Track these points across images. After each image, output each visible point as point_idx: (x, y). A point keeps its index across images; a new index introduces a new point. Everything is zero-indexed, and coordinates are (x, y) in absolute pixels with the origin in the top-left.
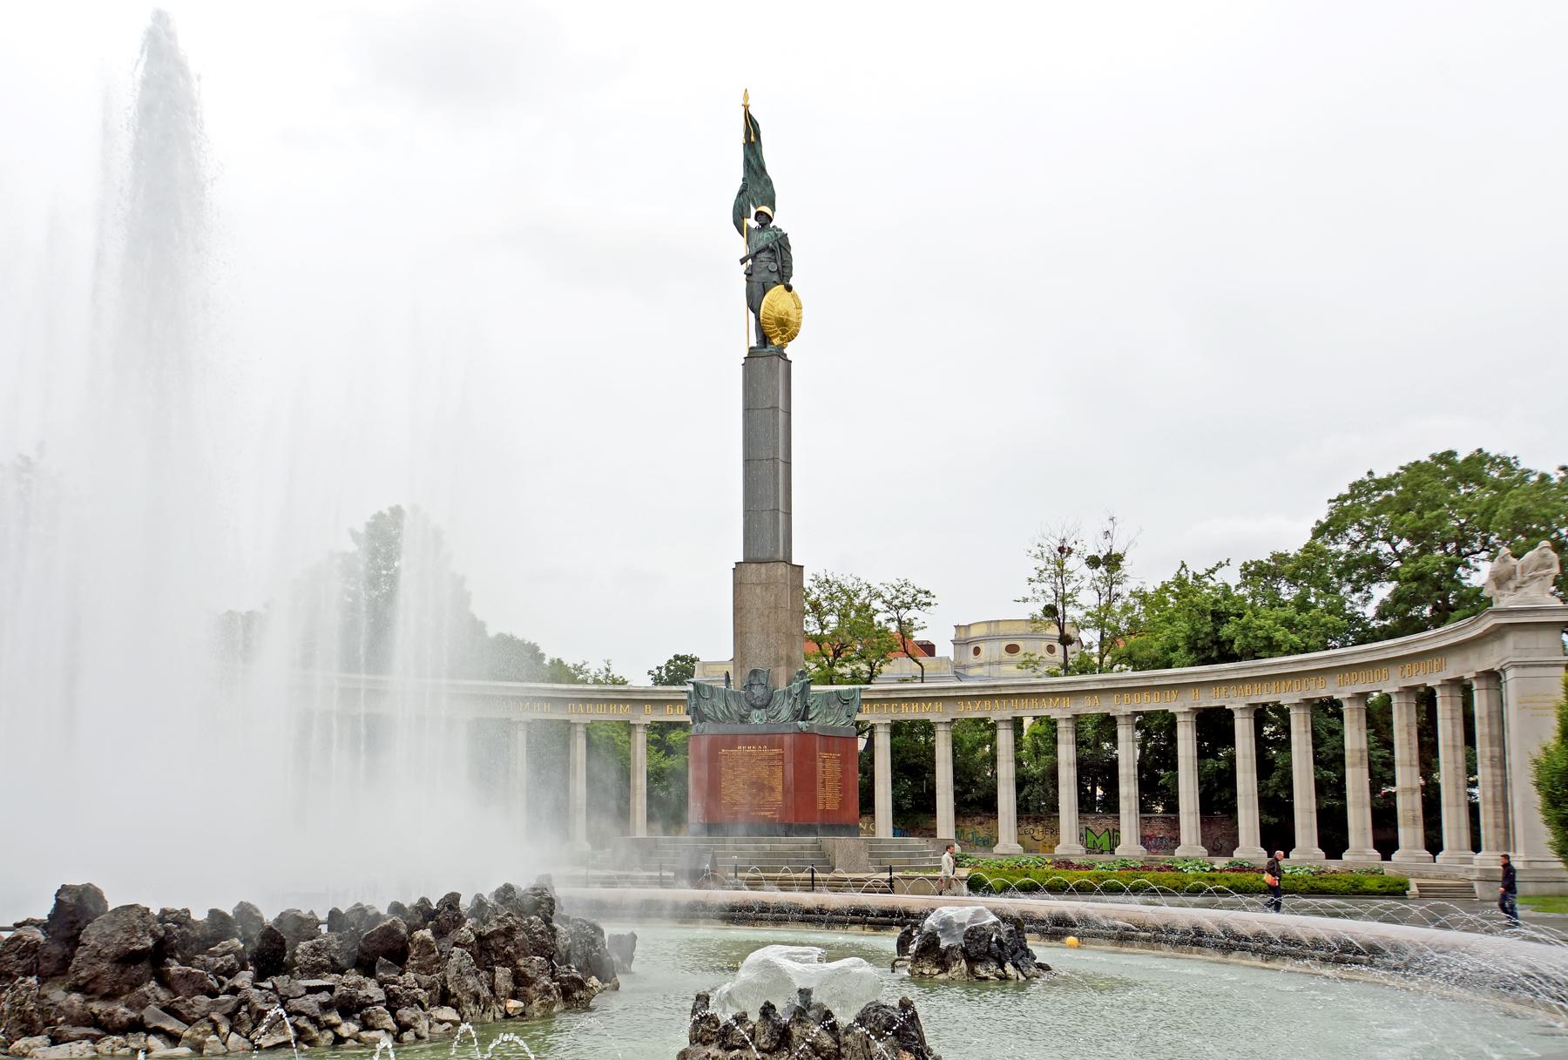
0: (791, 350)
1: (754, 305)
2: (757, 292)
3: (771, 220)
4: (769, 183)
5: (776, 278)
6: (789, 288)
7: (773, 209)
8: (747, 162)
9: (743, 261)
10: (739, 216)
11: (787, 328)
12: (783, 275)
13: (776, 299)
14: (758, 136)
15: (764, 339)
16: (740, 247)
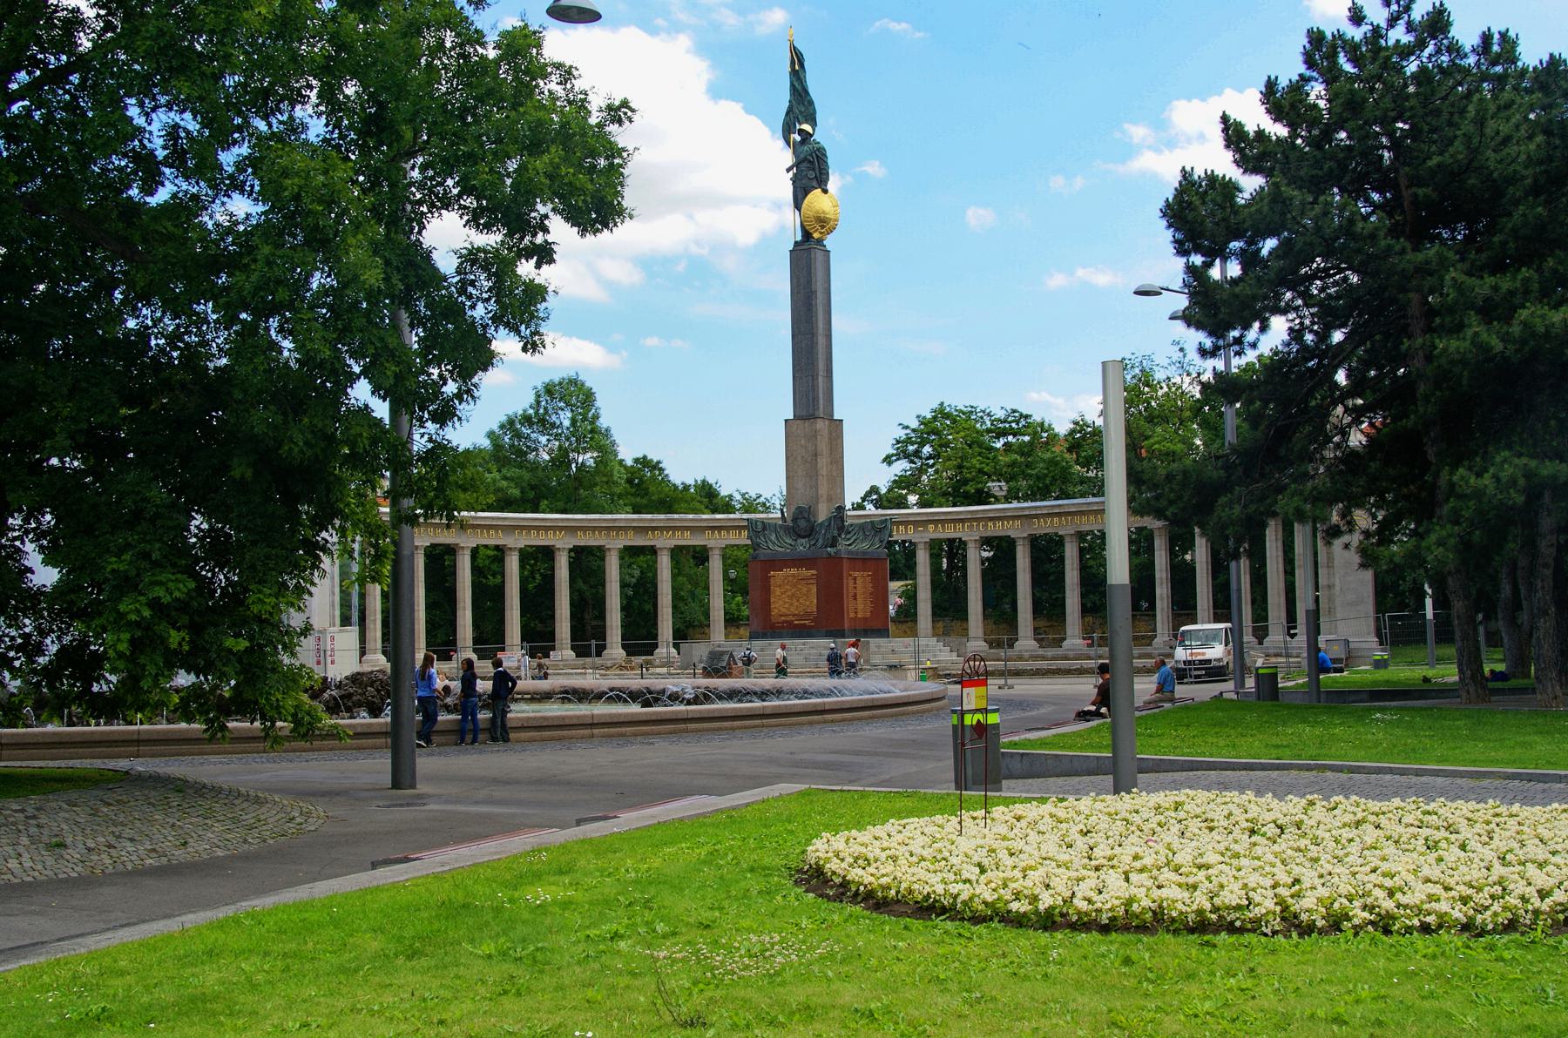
0: (830, 242)
1: (798, 205)
2: (800, 196)
3: (811, 136)
4: (811, 103)
5: (815, 184)
6: (825, 191)
7: (814, 124)
8: (792, 85)
9: (788, 170)
10: (788, 129)
11: (825, 223)
12: (821, 181)
13: (816, 200)
14: (802, 65)
15: (807, 235)
16: (788, 158)
